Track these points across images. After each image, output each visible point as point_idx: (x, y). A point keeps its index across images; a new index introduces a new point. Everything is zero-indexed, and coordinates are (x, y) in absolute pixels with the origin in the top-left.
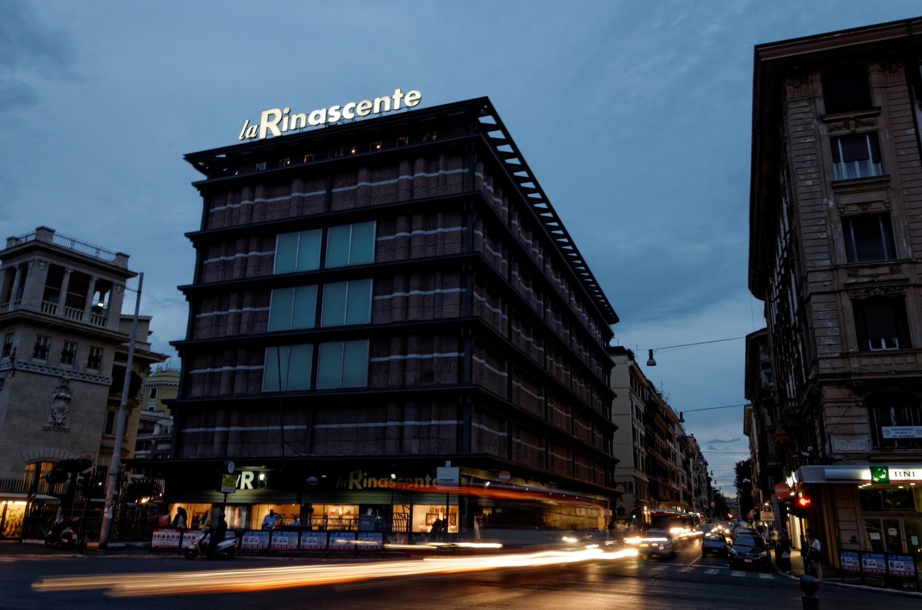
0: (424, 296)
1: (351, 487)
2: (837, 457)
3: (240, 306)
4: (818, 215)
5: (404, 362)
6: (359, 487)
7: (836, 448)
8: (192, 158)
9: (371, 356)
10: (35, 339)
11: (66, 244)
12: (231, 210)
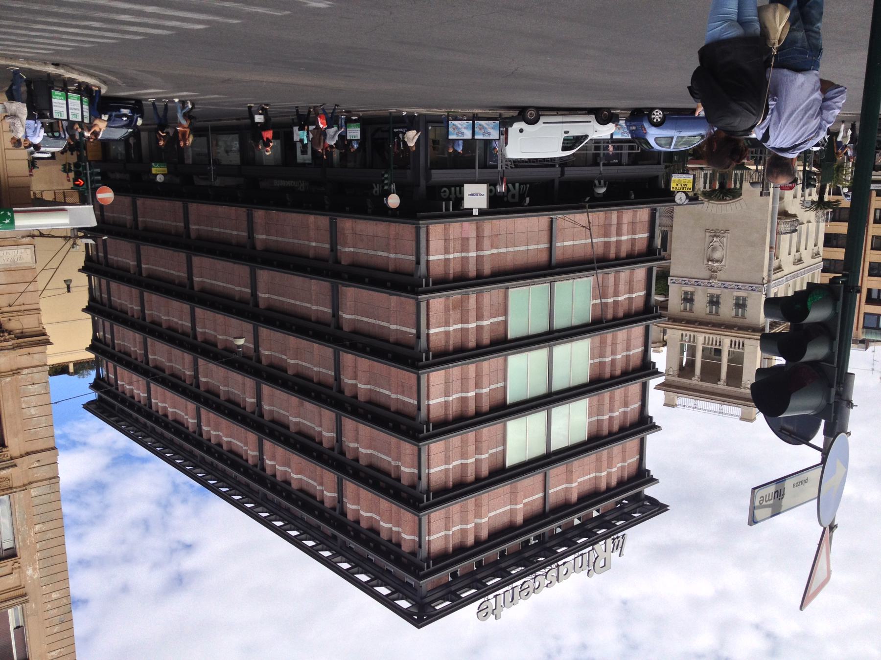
0: (462, 391)
1: (517, 185)
2: (27, 240)
3: (613, 361)
4: (46, 554)
5: (479, 317)
6: (510, 185)
7: (29, 251)
8: (657, 508)
9: (505, 322)
10: (747, 314)
11: (727, 408)
12: (624, 461)
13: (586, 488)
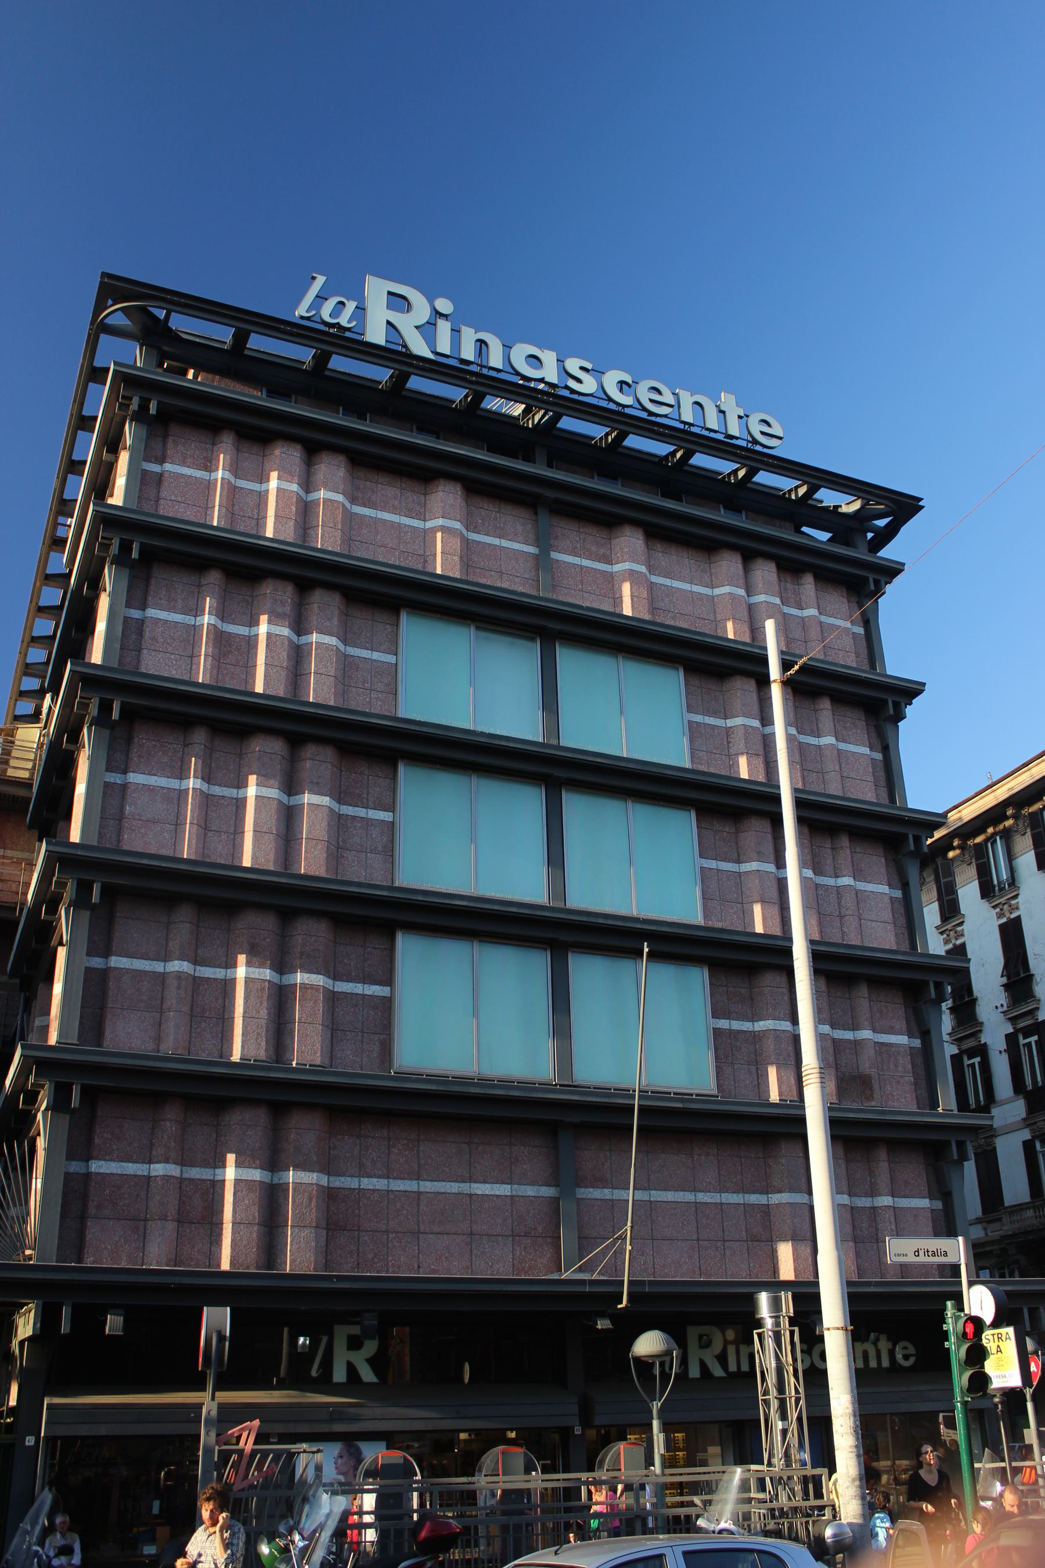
6: (718, 1372)
13: (388, 489)
